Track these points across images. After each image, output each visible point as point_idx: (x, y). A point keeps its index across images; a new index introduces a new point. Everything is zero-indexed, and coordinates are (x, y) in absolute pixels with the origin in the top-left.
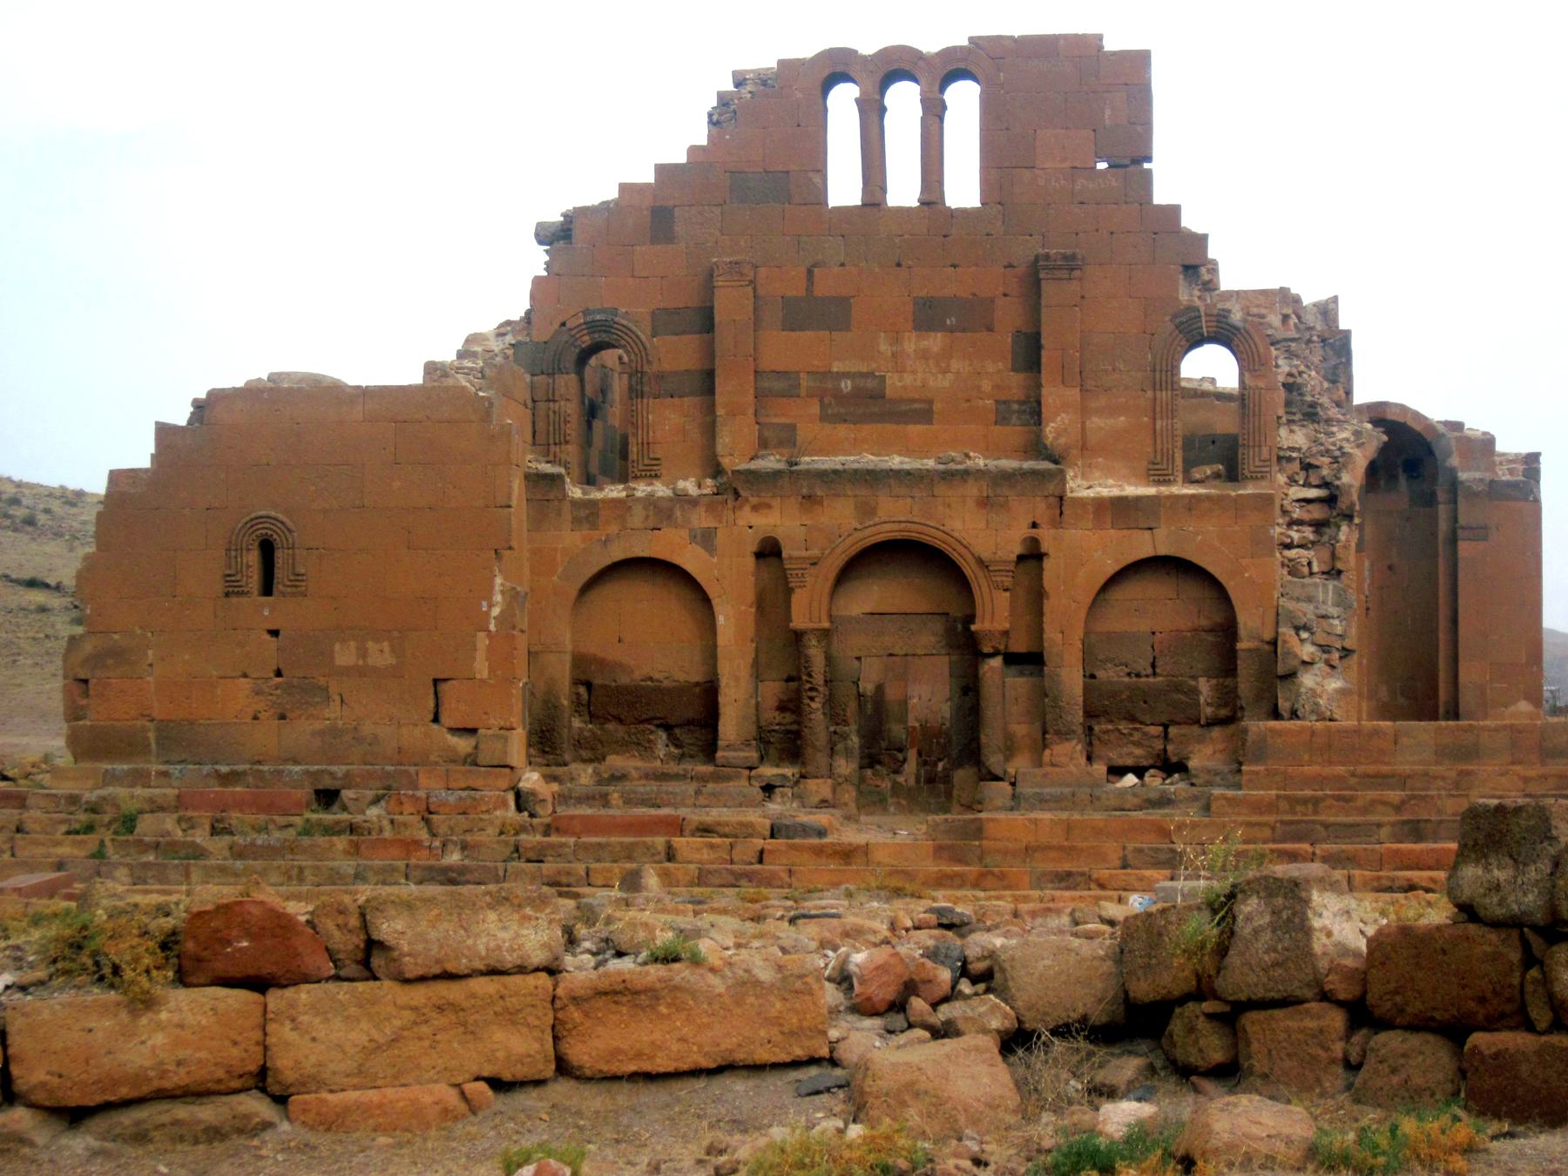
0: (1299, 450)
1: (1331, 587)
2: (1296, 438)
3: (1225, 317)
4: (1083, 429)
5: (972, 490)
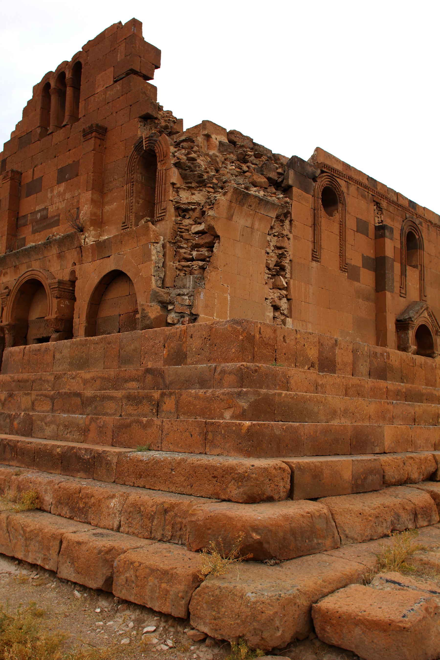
0: (199, 204)
1: (192, 277)
2: (194, 197)
3: (152, 137)
4: (102, 213)
5: (54, 251)
